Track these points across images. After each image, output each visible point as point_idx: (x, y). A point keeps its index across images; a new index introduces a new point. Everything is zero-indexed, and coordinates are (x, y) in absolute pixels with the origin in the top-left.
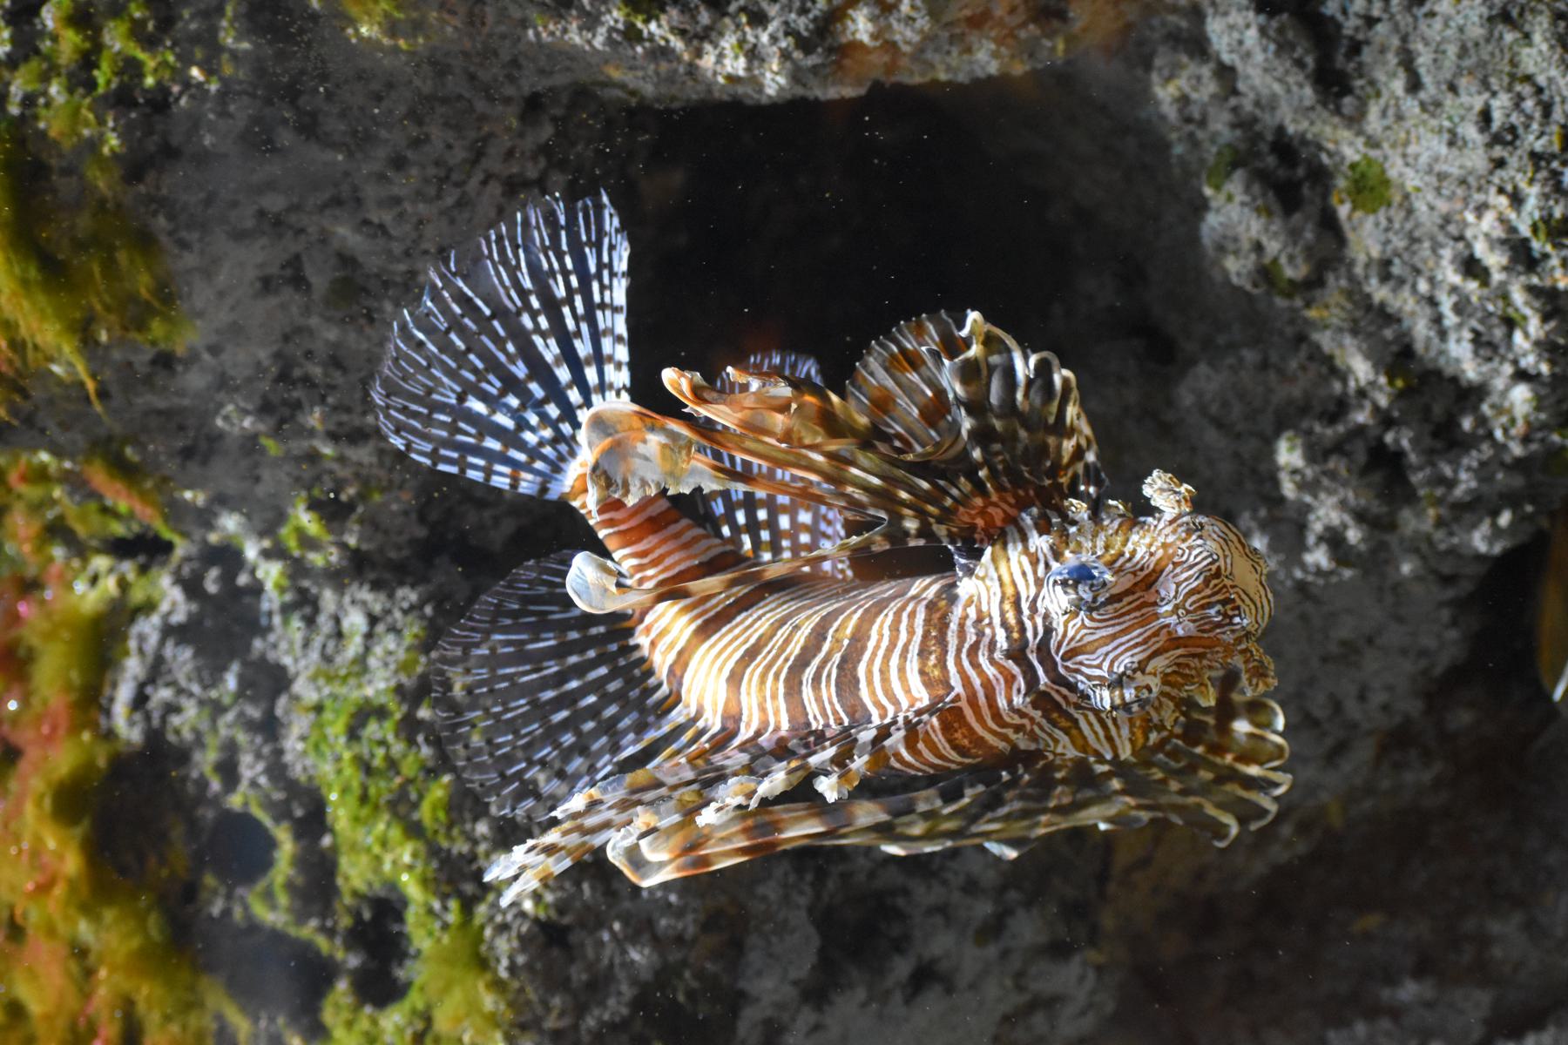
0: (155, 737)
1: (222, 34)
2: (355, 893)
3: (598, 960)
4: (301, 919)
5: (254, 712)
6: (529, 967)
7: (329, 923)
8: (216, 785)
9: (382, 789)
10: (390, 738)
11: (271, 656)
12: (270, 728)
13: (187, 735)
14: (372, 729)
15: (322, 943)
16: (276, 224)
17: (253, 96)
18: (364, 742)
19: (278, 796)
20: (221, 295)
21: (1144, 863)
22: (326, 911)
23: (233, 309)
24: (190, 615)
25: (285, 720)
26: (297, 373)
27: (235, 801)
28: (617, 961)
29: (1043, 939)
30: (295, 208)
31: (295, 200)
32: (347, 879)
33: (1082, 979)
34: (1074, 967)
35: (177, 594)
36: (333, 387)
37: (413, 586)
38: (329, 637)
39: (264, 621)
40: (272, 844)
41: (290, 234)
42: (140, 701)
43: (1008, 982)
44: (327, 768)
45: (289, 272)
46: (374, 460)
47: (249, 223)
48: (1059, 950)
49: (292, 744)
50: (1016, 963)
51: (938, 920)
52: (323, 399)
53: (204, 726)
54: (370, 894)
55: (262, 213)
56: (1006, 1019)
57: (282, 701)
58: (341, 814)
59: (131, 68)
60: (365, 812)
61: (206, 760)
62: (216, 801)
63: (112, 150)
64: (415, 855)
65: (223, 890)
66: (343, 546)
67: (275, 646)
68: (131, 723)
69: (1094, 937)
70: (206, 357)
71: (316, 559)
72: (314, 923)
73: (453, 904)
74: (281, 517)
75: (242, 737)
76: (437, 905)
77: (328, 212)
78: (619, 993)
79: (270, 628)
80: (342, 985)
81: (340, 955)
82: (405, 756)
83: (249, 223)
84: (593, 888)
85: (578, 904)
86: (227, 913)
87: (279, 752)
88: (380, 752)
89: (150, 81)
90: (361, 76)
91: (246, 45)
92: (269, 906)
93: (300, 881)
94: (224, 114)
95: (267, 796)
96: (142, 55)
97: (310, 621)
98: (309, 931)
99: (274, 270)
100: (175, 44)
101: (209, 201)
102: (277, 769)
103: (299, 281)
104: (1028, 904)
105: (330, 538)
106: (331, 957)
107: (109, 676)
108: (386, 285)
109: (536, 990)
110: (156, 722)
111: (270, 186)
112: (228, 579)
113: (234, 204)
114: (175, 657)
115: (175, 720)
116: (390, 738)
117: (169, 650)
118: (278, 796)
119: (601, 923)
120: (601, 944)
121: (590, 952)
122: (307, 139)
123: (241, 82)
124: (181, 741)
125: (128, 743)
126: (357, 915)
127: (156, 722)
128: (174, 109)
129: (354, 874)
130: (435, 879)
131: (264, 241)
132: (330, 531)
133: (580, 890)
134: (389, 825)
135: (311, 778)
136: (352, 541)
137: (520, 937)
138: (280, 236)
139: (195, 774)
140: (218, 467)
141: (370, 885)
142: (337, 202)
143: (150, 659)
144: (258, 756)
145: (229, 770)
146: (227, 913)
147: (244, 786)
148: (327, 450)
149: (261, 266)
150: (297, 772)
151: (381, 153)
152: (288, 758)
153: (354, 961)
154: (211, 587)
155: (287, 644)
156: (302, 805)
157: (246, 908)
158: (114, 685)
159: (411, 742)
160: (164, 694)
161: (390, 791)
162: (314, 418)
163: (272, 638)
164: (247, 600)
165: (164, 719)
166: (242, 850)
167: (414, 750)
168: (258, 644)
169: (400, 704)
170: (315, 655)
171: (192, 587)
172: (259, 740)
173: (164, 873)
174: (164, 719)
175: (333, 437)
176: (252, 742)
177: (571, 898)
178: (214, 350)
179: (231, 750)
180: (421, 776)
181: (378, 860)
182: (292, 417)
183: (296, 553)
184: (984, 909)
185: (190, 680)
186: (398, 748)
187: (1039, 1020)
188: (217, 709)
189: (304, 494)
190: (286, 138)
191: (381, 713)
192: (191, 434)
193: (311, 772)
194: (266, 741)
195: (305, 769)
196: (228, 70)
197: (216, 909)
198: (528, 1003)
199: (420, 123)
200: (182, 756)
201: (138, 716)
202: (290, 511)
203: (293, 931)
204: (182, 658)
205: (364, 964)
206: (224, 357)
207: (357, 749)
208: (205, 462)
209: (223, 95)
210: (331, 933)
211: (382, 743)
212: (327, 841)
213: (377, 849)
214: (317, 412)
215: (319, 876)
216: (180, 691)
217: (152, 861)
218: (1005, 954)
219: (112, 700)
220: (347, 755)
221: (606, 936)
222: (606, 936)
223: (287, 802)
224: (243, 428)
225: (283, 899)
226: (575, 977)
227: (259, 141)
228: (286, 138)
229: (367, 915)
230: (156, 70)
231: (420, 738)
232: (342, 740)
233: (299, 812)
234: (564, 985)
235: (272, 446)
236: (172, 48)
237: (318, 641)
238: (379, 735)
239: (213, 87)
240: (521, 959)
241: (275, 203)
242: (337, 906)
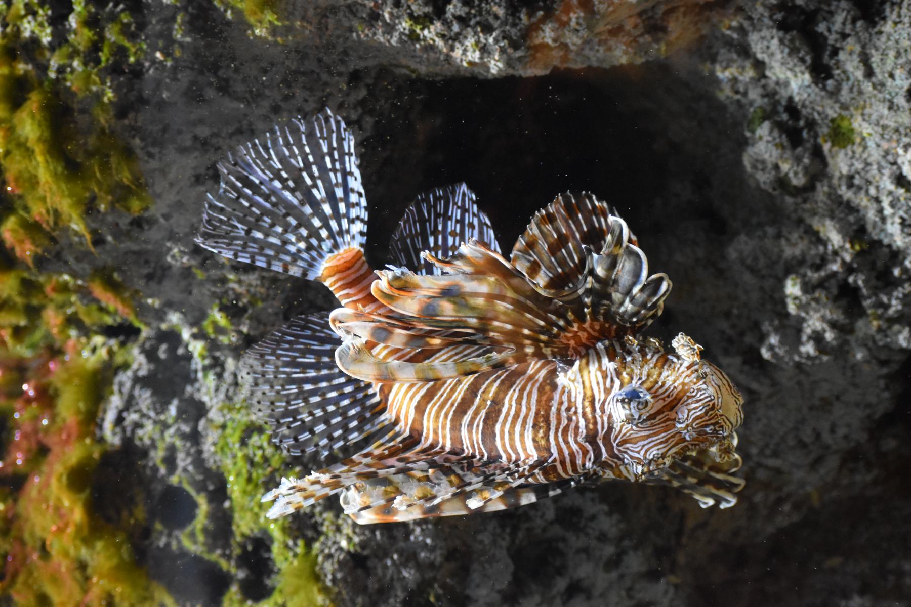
0: (128, 442)
1: (174, 33)
2: (243, 535)
3: (384, 575)
4: (211, 549)
5: (186, 429)
6: (344, 579)
7: (227, 552)
8: (163, 470)
10: (265, 444)
11: (197, 396)
12: (195, 437)
13: (147, 441)
14: (255, 439)
15: (224, 564)
16: (204, 144)
17: (192, 69)
18: (250, 447)
19: (199, 477)
20: (171, 185)
22: (226, 545)
23: (178, 193)
24: (149, 370)
25: (204, 433)
27: (174, 480)
28: (395, 577)
29: (643, 569)
30: (216, 135)
31: (215, 130)
32: (238, 526)
33: (666, 592)
35: (142, 359)
38: (230, 385)
39: (193, 376)
40: (195, 505)
41: (212, 150)
42: (119, 420)
43: (623, 593)
44: (228, 462)
45: (211, 172)
46: (259, 282)
47: (188, 143)
48: (653, 575)
49: (208, 447)
50: (628, 583)
51: (584, 556)
53: (157, 436)
54: (251, 535)
55: (196, 138)
57: (202, 424)
58: (235, 487)
59: (120, 52)
61: (157, 456)
62: (163, 479)
63: (109, 99)
65: (166, 532)
66: (240, 333)
67: (199, 390)
68: (114, 434)
70: (162, 220)
71: (224, 340)
73: (300, 543)
74: (203, 315)
75: (178, 443)
76: (291, 543)
77: (234, 138)
78: (396, 596)
79: (196, 380)
80: (234, 589)
81: (233, 570)
82: (273, 455)
83: (188, 143)
84: (382, 534)
85: (373, 543)
86: (168, 545)
87: (200, 452)
89: (132, 59)
90: (255, 59)
91: (188, 39)
92: (191, 541)
93: (211, 527)
94: (175, 79)
95: (192, 477)
96: (127, 44)
98: (215, 556)
99: (202, 171)
100: (147, 38)
101: (165, 130)
102: (199, 461)
104: (635, 548)
105: (232, 328)
106: (228, 572)
107: (102, 406)
109: (348, 593)
110: (128, 433)
111: (201, 122)
112: (172, 350)
113: (180, 132)
114: (140, 395)
115: (140, 432)
116: (265, 444)
117: (137, 392)
118: (199, 477)
119: (387, 555)
120: (386, 567)
121: (379, 571)
122: (223, 95)
123: (185, 61)
124: (143, 445)
125: (113, 445)
126: (243, 546)
127: (128, 433)
128: (146, 76)
130: (290, 528)
131: (197, 154)
132: (232, 324)
133: (375, 535)
135: (218, 467)
136: (245, 329)
137: (339, 562)
138: (206, 151)
139: (151, 464)
140: (167, 285)
141: (252, 530)
142: (239, 131)
143: (126, 396)
144: (188, 454)
145: (170, 461)
146: (168, 545)
147: (179, 471)
148: (231, 276)
149: (195, 168)
150: (211, 464)
151: (266, 104)
152: (205, 455)
153: (241, 574)
154: (162, 354)
155: (207, 389)
156: (213, 483)
157: (179, 542)
158: (105, 411)
160: (132, 417)
161: (265, 476)
163: (197, 385)
164: (182, 363)
165: (133, 431)
166: (175, 507)
167: (279, 452)
168: (189, 389)
170: (222, 396)
171: (151, 355)
172: (188, 444)
173: (132, 521)
174: (133, 431)
176: (184, 446)
177: (370, 540)
178: (167, 217)
179: (172, 449)
180: (283, 468)
181: (257, 516)
183: (212, 336)
184: (609, 550)
185: (149, 409)
186: (269, 451)
188: (165, 426)
189: (217, 301)
190: (210, 93)
191: (260, 430)
192: (153, 265)
193: (219, 464)
194: (192, 446)
195: (215, 462)
196: (178, 53)
197: (162, 542)
198: (343, 600)
199: (289, 86)
200: (144, 453)
201: (118, 430)
202: (209, 311)
203: (206, 557)
204: (145, 398)
205: (247, 576)
206: (172, 221)
207: (245, 451)
208: (160, 282)
209: (175, 68)
210: (228, 558)
211: (261, 447)
212: (227, 504)
213: (256, 510)
215: (222, 524)
216: (143, 415)
217: (125, 514)
218: (622, 576)
219: (103, 420)
220: (240, 454)
221: (389, 563)
222: (389, 563)
223: (204, 481)
224: (182, 263)
225: (201, 538)
226: (370, 585)
227: (195, 96)
228: (210, 93)
229: (250, 548)
230: (135, 53)
232: (237, 445)
233: (211, 487)
234: (364, 590)
235: (200, 275)
236: (145, 40)
238: (258, 444)
239: (169, 64)
240: (339, 575)
241: (203, 132)
242: (232, 542)
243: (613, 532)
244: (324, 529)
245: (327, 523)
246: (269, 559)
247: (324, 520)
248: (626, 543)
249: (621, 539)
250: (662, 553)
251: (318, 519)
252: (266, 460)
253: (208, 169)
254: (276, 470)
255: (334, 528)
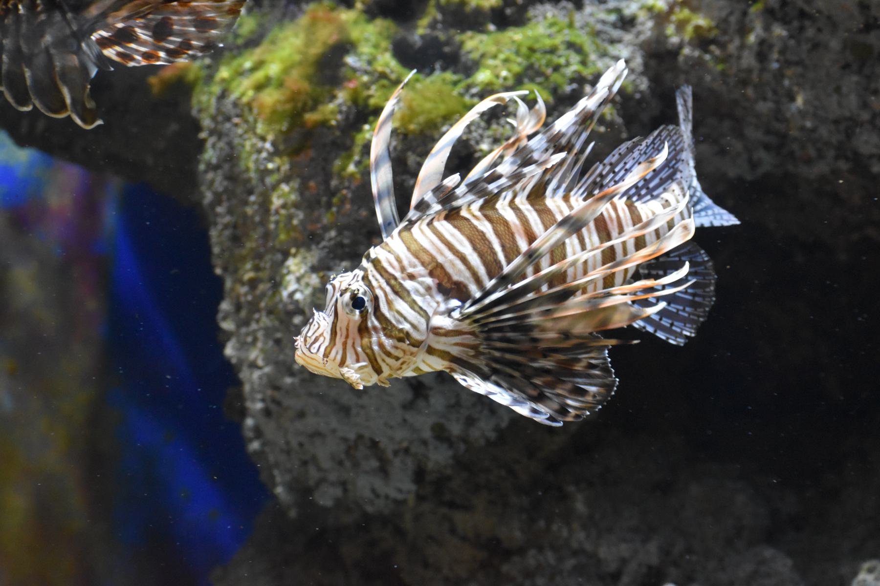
2: (462, 43)
9: (540, 61)
14: (575, 58)
21: (453, 531)
26: (807, 23)
29: (430, 466)
32: (471, 38)
33: (400, 491)
34: (409, 486)
36: (799, 43)
37: (649, 87)
43: (405, 444)
48: (419, 475)
50: (416, 448)
51: (453, 401)
52: (791, 37)
56: (374, 444)
57: (570, 6)
58: (516, 35)
60: (524, 50)
64: (505, 79)
66: (681, 46)
69: (420, 498)
72: (439, 17)
76: (474, 91)
88: (562, 61)
93: (468, 9)
97: (614, 26)
103: (868, 28)
104: (455, 457)
106: (415, 27)
108: (868, 78)
129: (473, 43)
134: (519, 64)
135: (529, 20)
136: (686, 51)
137: (468, 140)
141: (469, 52)
148: (752, 38)
150: (531, 13)
159: (572, 80)
161: (540, 66)
162: (779, 31)
169: (592, 74)
170: (599, 27)
175: (762, 42)
180: (552, 86)
181: (495, 57)
182: (776, 20)
183: (674, 18)
184: (455, 429)
187: (374, 463)
191: (584, 63)
193: (534, 21)
207: (562, 47)
211: (568, 64)
212: (492, 27)
213: (502, 56)
214: (784, 33)
218: (425, 443)
231: (575, 86)
232: (568, 38)
233: (508, 11)
237: (608, 29)
242: (452, 32)
243: (475, 433)
244: (494, 126)
245: (500, 130)
246: (432, 71)
247: (503, 127)
248: (462, 447)
249: (465, 440)
250: (441, 482)
251: (502, 121)
252: (557, 68)
253: (876, 19)
254: (547, 78)
255: (498, 136)
